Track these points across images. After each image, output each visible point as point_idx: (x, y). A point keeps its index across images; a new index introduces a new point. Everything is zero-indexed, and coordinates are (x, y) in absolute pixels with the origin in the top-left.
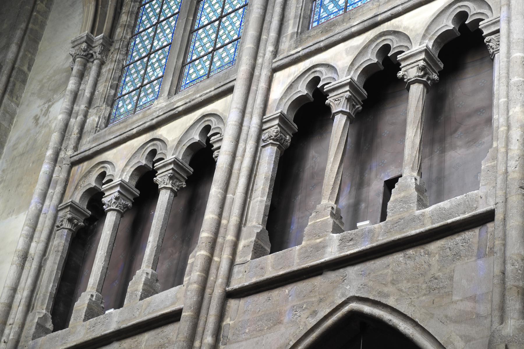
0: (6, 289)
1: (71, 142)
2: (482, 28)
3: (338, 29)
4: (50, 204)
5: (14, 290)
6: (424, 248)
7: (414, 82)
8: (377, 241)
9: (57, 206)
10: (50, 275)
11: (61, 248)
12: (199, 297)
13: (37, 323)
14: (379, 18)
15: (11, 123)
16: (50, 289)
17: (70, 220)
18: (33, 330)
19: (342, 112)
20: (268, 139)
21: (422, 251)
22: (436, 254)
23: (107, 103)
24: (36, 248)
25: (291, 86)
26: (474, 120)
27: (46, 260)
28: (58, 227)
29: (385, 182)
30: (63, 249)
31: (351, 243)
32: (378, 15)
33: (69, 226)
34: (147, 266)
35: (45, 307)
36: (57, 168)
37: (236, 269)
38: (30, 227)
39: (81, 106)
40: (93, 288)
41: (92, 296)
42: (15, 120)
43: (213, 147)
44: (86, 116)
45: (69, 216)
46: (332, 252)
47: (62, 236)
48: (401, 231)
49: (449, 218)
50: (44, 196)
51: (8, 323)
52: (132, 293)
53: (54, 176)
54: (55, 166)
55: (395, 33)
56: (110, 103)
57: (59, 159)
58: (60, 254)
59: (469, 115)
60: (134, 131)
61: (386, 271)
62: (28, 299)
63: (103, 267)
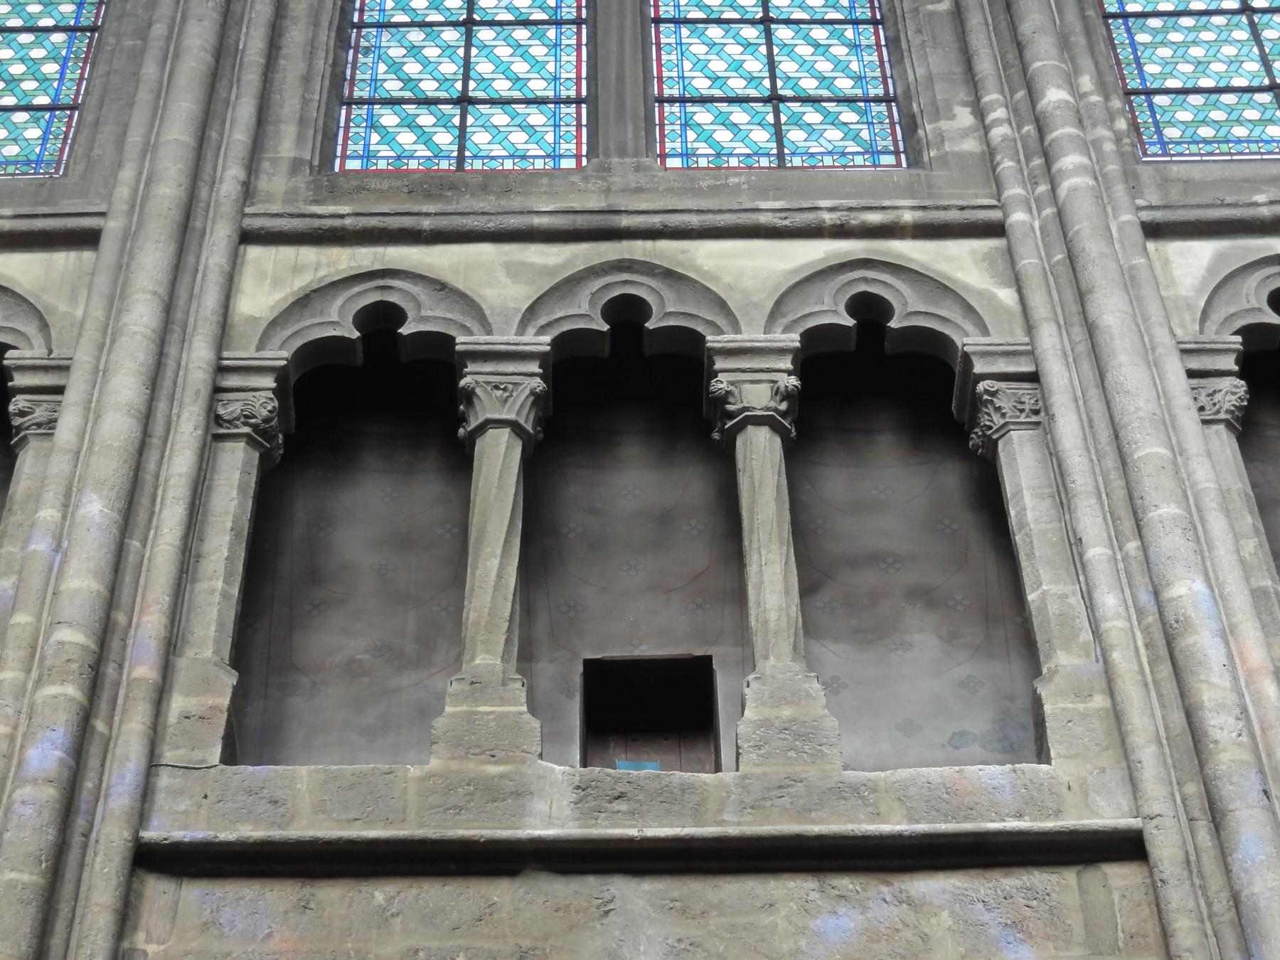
2: (974, 353)
3: (468, 203)
6: (888, 884)
7: (758, 421)
8: (721, 823)
14: (625, 222)
19: (515, 426)
20: (237, 419)
21: (884, 889)
22: (942, 908)
25: (304, 302)
26: (868, 579)
29: (588, 664)
31: (622, 806)
32: (619, 212)
37: (164, 780)
43: (12, 380)
46: (551, 816)
48: (803, 813)
49: (967, 819)
55: (670, 275)
59: (854, 563)
61: (766, 920)
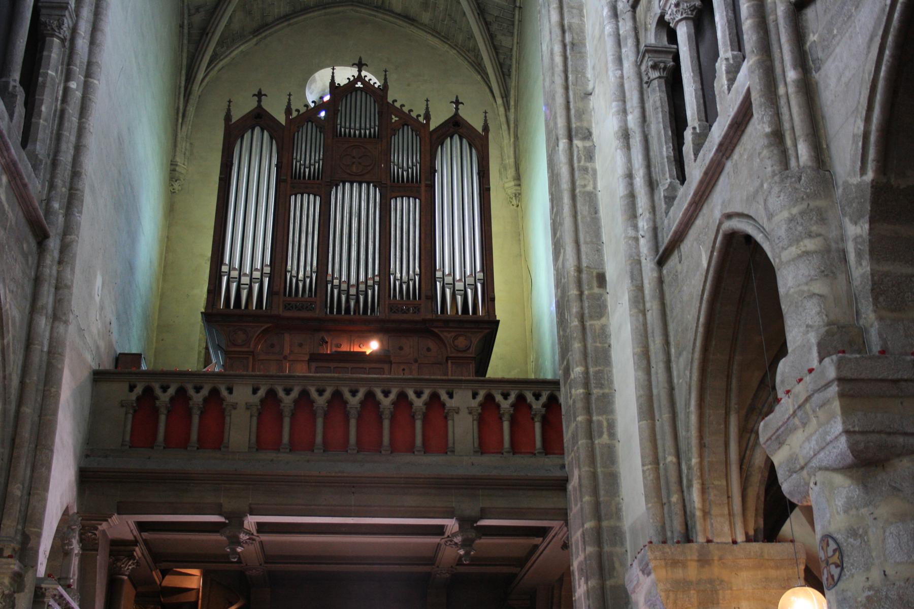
0: (621, 180)
5: (630, 176)
9: (636, 61)
10: (659, 138)
11: (658, 104)
12: (758, 33)
13: (665, 197)
15: (581, 15)
16: (665, 153)
17: (655, 67)
18: (664, 206)
24: (633, 120)
27: (648, 126)
28: (647, 83)
33: (654, 74)
34: (726, 51)
35: (668, 175)
36: (620, 24)
38: (618, 101)
40: (693, 120)
41: (694, 128)
45: (650, 63)
47: (654, 90)
50: (619, 60)
51: (638, 214)
52: (720, 93)
53: (621, 32)
54: (617, 21)
58: (660, 110)
62: (647, 177)
63: (695, 90)
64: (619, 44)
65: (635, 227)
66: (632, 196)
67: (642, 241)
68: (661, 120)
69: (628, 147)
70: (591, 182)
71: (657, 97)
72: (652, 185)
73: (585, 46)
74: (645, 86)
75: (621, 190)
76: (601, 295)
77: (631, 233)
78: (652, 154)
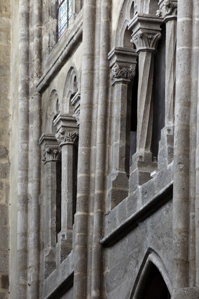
1: (34, 69)
4: (33, 139)
5: (25, 234)
9: (38, 141)
11: (49, 182)
12: (81, 256)
17: (50, 152)
23: (52, 16)
24: (32, 187)
28: (43, 160)
30: (52, 182)
35: (50, 243)
36: (30, 100)
38: (22, 170)
39: (34, 28)
42: (11, 34)
44: (40, 36)
45: (47, 150)
47: (47, 170)
51: (28, 266)
53: (30, 109)
54: (28, 99)
56: (54, 14)
57: (30, 91)
58: (50, 188)
60: (60, 60)
62: (36, 240)
63: (68, 204)
64: (27, 120)
65: (25, 276)
66: (25, 251)
67: (29, 289)
68: (50, 197)
69: (26, 210)
70: (4, 197)
71: (48, 176)
72: (39, 246)
73: (9, 68)
74: (43, 162)
75: (19, 246)
76: (4, 294)
77: (22, 281)
78: (42, 220)
